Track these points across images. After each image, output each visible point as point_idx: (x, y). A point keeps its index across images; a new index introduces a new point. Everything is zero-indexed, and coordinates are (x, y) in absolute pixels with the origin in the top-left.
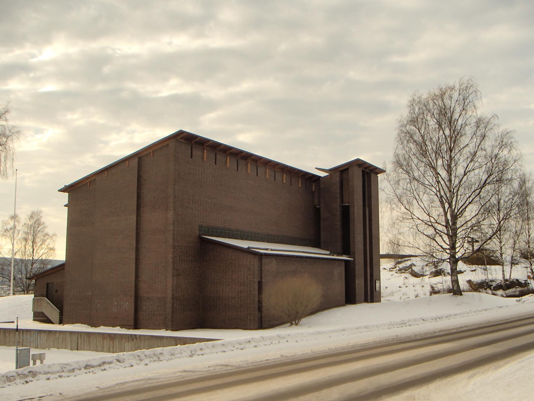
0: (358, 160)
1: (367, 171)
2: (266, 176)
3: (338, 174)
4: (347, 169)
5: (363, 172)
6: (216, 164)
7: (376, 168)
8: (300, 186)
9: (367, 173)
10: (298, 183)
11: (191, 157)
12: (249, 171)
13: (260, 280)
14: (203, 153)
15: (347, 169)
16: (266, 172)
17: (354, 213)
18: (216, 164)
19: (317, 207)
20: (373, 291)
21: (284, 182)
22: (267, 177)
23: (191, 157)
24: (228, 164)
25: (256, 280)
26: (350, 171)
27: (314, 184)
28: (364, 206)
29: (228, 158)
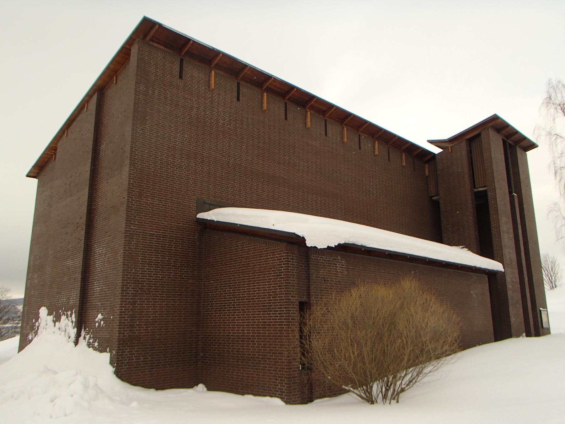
0: (495, 119)
1: (509, 141)
2: (342, 139)
3: (464, 144)
4: (479, 135)
5: (504, 142)
6: (238, 99)
7: (524, 138)
8: (404, 164)
9: (510, 144)
10: (402, 159)
11: (181, 77)
12: (309, 124)
13: (304, 299)
14: (210, 77)
15: (479, 135)
16: (342, 134)
17: (496, 199)
18: (238, 99)
19: (434, 198)
20: (539, 329)
21: (377, 153)
22: (345, 140)
23: (181, 77)
24: (265, 105)
25: (295, 299)
26: (482, 136)
27: (427, 166)
28: (510, 193)
29: (265, 94)
